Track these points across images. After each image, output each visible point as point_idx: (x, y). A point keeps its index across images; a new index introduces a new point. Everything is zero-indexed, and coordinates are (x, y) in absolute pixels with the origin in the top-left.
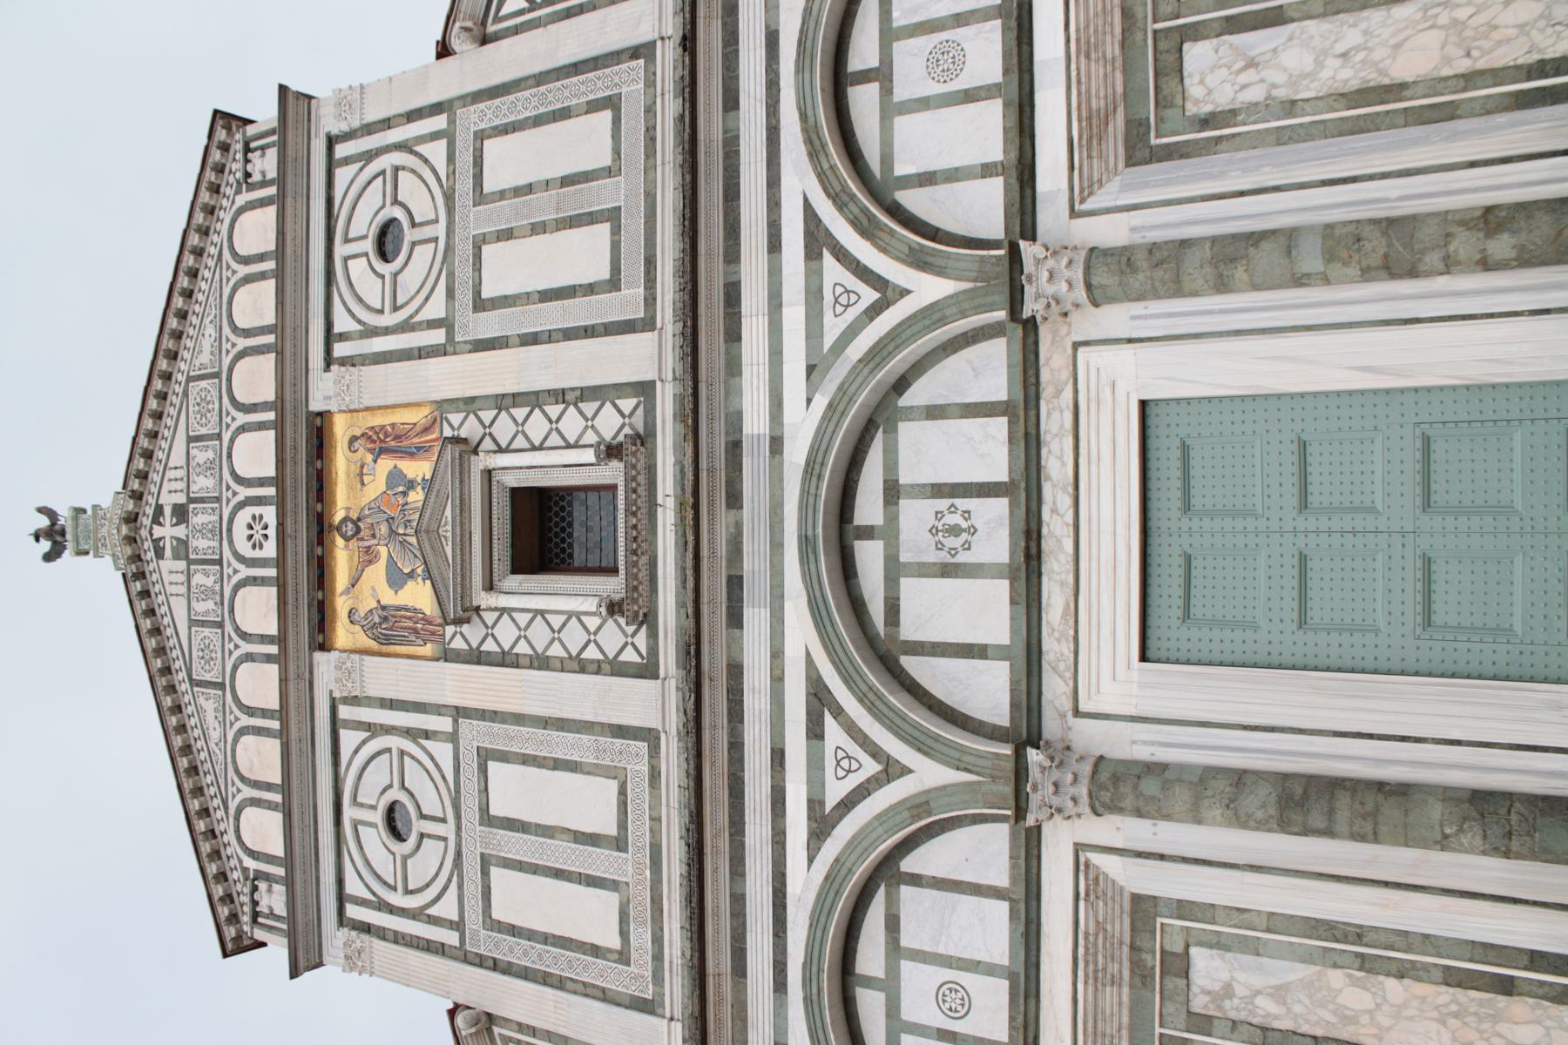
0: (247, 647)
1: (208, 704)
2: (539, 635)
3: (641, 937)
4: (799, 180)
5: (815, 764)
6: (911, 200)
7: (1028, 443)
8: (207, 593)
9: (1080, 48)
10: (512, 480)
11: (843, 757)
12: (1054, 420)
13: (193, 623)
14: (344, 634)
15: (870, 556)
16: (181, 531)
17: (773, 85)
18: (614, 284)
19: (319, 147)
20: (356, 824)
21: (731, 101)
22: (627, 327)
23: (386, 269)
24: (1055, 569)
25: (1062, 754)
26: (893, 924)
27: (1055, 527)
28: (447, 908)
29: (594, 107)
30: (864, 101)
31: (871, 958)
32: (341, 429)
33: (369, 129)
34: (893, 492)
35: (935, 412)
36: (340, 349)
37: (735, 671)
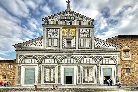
0: (62, 21)
1: (57, 18)
2: (64, 42)
3: (49, 47)
4: (84, 56)
5: (59, 56)
6: (83, 60)
7: (72, 64)
8: (65, 18)
9: (88, 66)
10: (71, 41)
11: (59, 57)
12: (73, 65)
13: (63, 17)
14: (63, 30)
15: (68, 58)
16: (69, 16)
17: (88, 55)
18: (80, 47)
19: (91, 28)
20: (52, 30)
21: (88, 53)
22: (78, 47)
23: (83, 33)
24: (68, 65)
25: (60, 65)
26: (52, 59)
27: (69, 65)
28: (49, 36)
29: (89, 46)
30: (87, 58)
31: (50, 58)
32: (75, 30)
33: (91, 32)
34: (71, 59)
35: (74, 61)
36: (79, 30)
37: (63, 52)
